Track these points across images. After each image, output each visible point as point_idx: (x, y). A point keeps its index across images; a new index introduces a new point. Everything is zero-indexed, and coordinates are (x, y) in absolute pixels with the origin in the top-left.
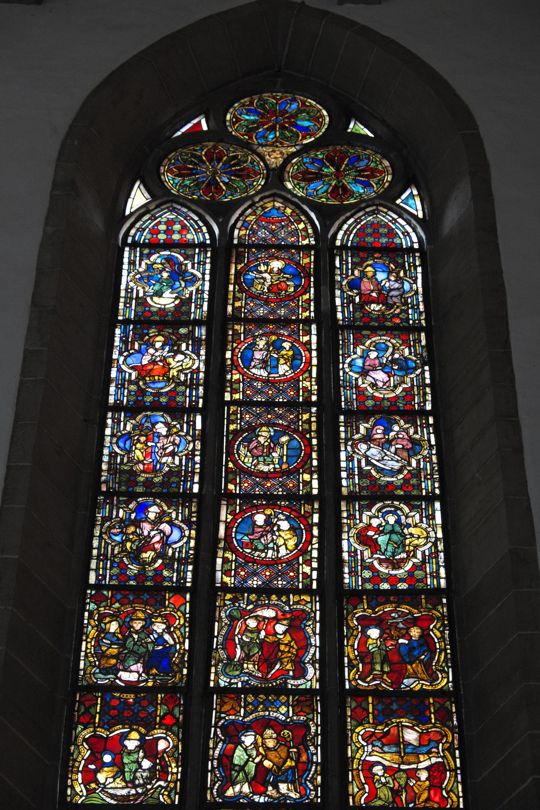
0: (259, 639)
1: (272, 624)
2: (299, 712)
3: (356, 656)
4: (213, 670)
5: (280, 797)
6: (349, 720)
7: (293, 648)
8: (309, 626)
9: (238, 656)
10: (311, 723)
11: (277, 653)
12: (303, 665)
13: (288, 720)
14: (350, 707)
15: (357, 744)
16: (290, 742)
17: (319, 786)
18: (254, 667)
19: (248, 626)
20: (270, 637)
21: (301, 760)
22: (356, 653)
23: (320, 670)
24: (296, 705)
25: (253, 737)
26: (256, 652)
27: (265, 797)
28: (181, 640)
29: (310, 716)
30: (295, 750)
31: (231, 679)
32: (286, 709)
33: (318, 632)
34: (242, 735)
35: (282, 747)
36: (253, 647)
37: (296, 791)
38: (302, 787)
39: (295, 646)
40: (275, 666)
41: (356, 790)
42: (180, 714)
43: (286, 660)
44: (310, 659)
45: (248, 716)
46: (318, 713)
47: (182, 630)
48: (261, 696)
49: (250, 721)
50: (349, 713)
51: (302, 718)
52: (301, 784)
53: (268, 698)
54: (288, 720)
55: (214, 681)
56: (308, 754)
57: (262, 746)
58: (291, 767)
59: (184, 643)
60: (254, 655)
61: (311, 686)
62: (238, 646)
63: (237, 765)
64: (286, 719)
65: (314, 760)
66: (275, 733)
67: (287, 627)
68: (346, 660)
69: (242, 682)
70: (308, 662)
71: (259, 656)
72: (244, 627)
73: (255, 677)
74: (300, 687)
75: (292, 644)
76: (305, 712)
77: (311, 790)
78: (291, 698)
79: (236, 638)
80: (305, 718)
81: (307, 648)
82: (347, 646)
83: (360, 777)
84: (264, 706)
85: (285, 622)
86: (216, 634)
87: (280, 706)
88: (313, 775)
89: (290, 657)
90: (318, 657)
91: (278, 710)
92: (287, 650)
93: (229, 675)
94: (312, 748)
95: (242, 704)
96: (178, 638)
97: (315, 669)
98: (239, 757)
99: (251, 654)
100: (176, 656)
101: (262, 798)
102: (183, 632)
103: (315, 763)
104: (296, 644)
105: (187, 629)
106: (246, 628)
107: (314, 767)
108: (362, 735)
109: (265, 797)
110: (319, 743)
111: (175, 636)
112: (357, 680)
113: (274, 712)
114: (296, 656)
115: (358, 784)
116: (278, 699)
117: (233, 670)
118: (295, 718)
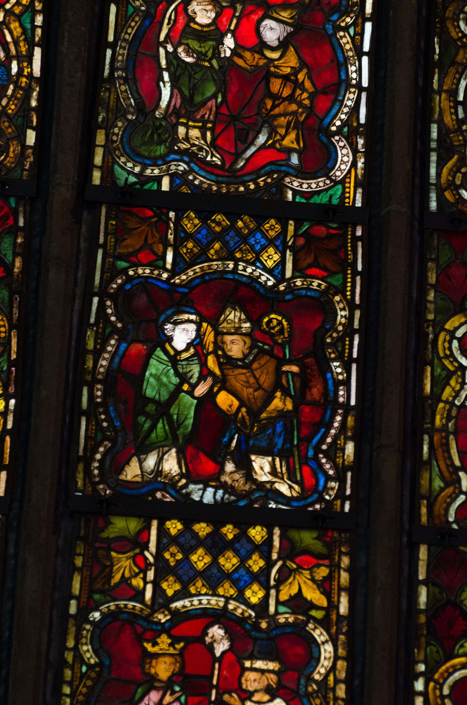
0: (219, 59)
1: (255, 17)
2: (309, 266)
3: (461, 122)
4: (101, 138)
5: (251, 492)
6: (431, 296)
7: (304, 90)
8: (346, 29)
9: (164, 103)
10: (337, 298)
11: (262, 103)
12: (325, 139)
13: (282, 288)
14: (436, 260)
15: (446, 363)
16: (282, 346)
17: (350, 468)
18: (204, 137)
19: (193, 19)
20: (248, 55)
21: (309, 398)
22: (461, 115)
23: (366, 155)
24: (302, 247)
25: (193, 327)
26: (209, 94)
27: (217, 488)
28: (24, 49)
29: (336, 281)
30: (295, 369)
31: (144, 167)
32: (276, 257)
33: (366, 47)
34: (167, 321)
35: (266, 358)
36: (204, 80)
37: (292, 477)
38: (306, 469)
39: (308, 84)
40: (256, 137)
41: (438, 483)
42: (15, 255)
43: (283, 120)
44: (345, 123)
45: (184, 271)
46: (355, 273)
47: (26, 19)
48: (219, 217)
49: (188, 284)
50: (432, 278)
51: (316, 283)
52: (304, 460)
53: (234, 223)
54: (282, 288)
55: (100, 168)
56: (325, 381)
57: (215, 352)
58: (282, 414)
59: (30, 58)
60: (204, 103)
61: (343, 197)
62: (166, 76)
63: (152, 400)
64: (276, 285)
65: (341, 400)
66: (248, 319)
67: (290, 29)
68: (434, 128)
69: (173, 177)
70: (339, 131)
71: (217, 107)
72: (182, 20)
73: (203, 163)
74: (316, 200)
75: (301, 76)
76: (324, 268)
77: (328, 478)
78: (291, 228)
79: (162, 51)
80: (324, 285)
81: (337, 92)
82: (439, 93)
83: (448, 451)
84: (225, 244)
85: (285, 15)
86: (111, 38)
87: (264, 248)
88: (336, 438)
89: (294, 113)
90: (362, 120)
91: (258, 259)
92: (286, 92)
93: (139, 155)
94: (335, 365)
95: (171, 237)
96: (16, 43)
97: (355, 151)
98: (157, 378)
99: (198, 99)
100: (10, 92)
101: (210, 491)
102: (28, 26)
103: (342, 406)
104: (310, 78)
105: (39, 20)
106: (187, 25)
107: (339, 418)
108: (459, 340)
109: (217, 488)
110: (355, 355)
111: (9, 38)
112: (458, 188)
113: (248, 262)
114: (310, 110)
115: (443, 468)
116: (258, 229)
117: (151, 142)
118: (299, 283)
